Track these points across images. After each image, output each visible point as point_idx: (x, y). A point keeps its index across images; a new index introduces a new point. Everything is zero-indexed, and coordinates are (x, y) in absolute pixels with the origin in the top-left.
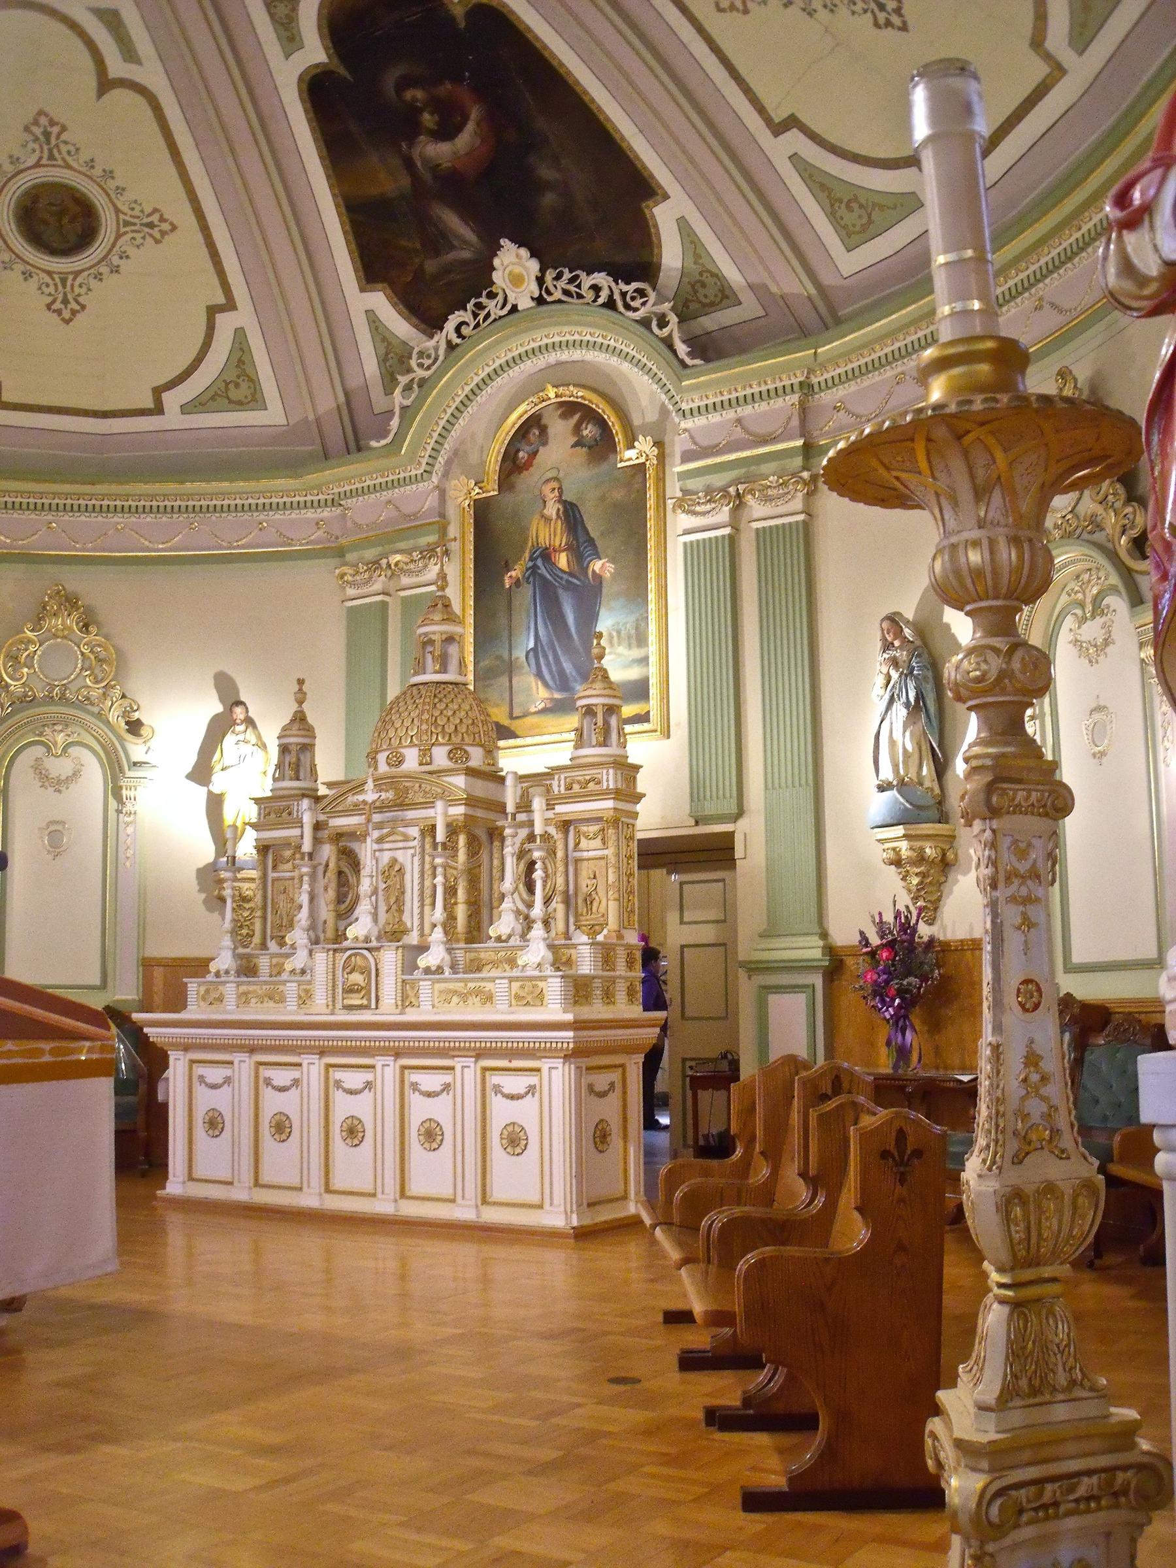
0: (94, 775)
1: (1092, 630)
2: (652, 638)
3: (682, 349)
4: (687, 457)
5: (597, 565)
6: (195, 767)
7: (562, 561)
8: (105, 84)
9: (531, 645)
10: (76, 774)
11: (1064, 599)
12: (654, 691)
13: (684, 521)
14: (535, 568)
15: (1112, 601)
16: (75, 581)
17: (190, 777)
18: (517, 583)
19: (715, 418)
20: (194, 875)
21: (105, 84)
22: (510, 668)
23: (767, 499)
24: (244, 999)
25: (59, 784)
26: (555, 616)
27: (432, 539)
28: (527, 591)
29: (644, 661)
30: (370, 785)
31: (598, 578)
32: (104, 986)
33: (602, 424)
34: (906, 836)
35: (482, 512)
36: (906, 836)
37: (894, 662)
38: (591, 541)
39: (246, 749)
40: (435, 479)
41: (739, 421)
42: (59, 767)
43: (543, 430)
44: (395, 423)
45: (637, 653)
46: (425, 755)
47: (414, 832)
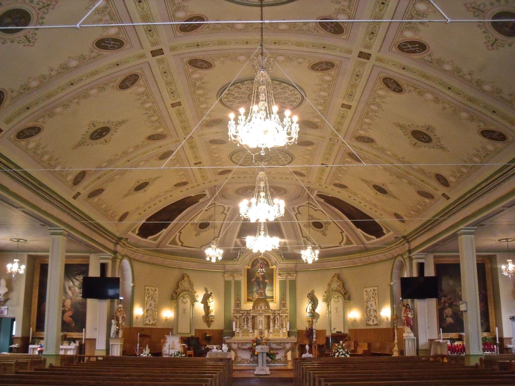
0: (189, 302)
1: (336, 300)
2: (274, 291)
3: (283, 257)
4: (279, 269)
5: (266, 280)
6: (202, 301)
7: (261, 279)
8: (222, 213)
9: (256, 289)
10: (187, 302)
11: (333, 296)
12: (274, 298)
13: (280, 277)
14: (257, 280)
15: (340, 298)
16: (190, 274)
17: (201, 303)
18: (254, 281)
19: (284, 265)
20: (202, 318)
21: (222, 213)
22: (253, 292)
23: (291, 276)
24: (243, 336)
25: (185, 303)
26: (259, 286)
27: (240, 273)
28: (255, 283)
29: (273, 294)
30: (261, 311)
31: (266, 283)
32: (190, 333)
33: (267, 262)
34: (311, 319)
35: (248, 270)
36: (311, 319)
37: (309, 299)
38: (265, 277)
39: (213, 300)
40: (241, 265)
41: (287, 266)
42: (185, 300)
43: (258, 261)
44: (238, 257)
45: (272, 293)
46: (265, 307)
47: (264, 316)
